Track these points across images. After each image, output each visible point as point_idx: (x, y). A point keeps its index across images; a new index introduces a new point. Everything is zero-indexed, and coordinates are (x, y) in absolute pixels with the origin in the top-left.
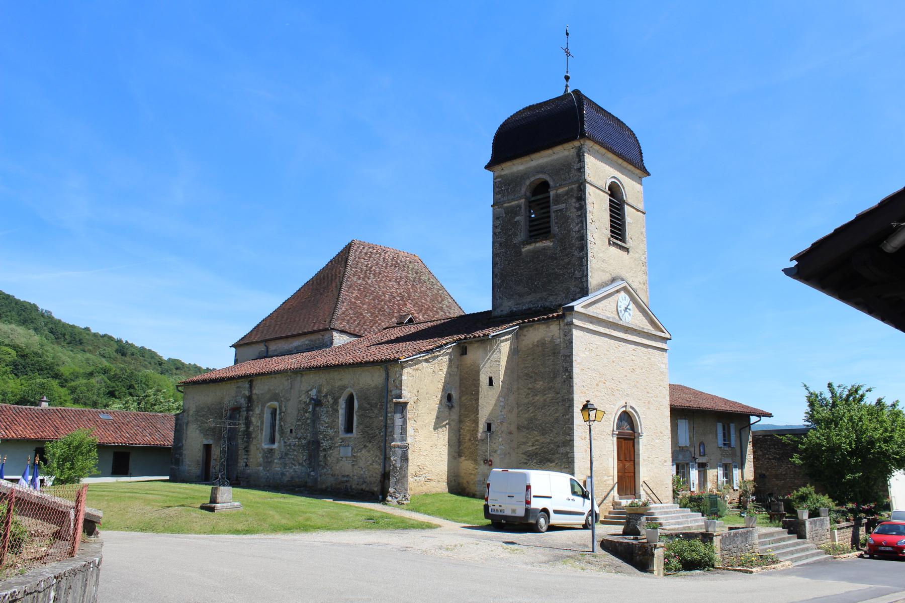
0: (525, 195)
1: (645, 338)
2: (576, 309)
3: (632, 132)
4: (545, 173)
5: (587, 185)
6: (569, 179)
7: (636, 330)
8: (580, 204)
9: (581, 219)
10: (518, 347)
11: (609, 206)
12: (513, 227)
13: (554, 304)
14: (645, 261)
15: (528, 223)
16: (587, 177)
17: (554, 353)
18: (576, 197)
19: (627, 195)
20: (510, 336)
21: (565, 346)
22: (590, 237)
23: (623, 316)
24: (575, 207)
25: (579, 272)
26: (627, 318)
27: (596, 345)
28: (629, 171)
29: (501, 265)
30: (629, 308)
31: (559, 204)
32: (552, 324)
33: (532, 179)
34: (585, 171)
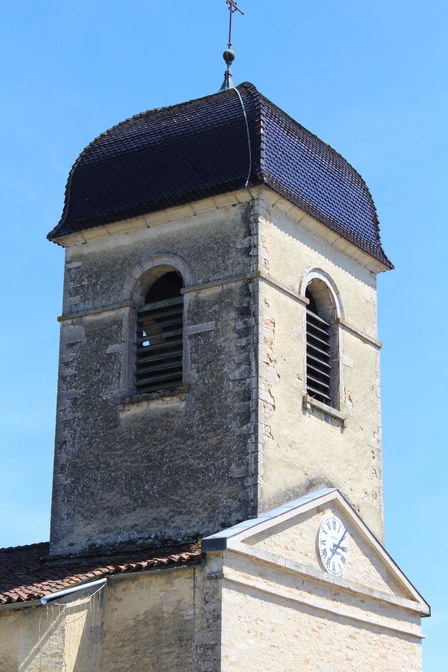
0: (131, 300)
1: (375, 612)
2: (230, 544)
3: (360, 176)
4: (175, 254)
5: (262, 285)
6: (225, 269)
7: (356, 593)
8: (245, 323)
9: (246, 354)
10: (103, 623)
11: (305, 329)
12: (103, 365)
13: (183, 532)
14: (378, 447)
15: (134, 359)
16: (261, 267)
17: (181, 640)
18: (237, 309)
19: (345, 309)
20: (87, 600)
21: (205, 625)
22: (263, 394)
23: (328, 563)
24: (234, 329)
25: (239, 466)
26: (337, 567)
27: (271, 623)
28: (351, 257)
29: (73, 445)
30: (342, 545)
31: (201, 321)
32: (179, 577)
33: (148, 266)
34: (257, 256)
